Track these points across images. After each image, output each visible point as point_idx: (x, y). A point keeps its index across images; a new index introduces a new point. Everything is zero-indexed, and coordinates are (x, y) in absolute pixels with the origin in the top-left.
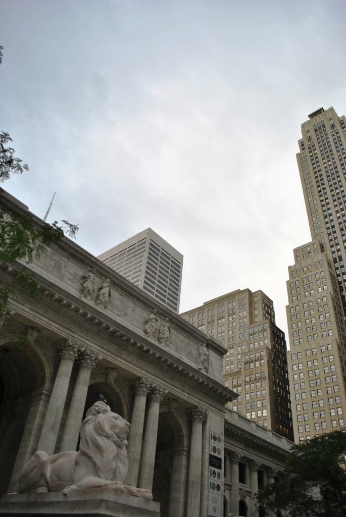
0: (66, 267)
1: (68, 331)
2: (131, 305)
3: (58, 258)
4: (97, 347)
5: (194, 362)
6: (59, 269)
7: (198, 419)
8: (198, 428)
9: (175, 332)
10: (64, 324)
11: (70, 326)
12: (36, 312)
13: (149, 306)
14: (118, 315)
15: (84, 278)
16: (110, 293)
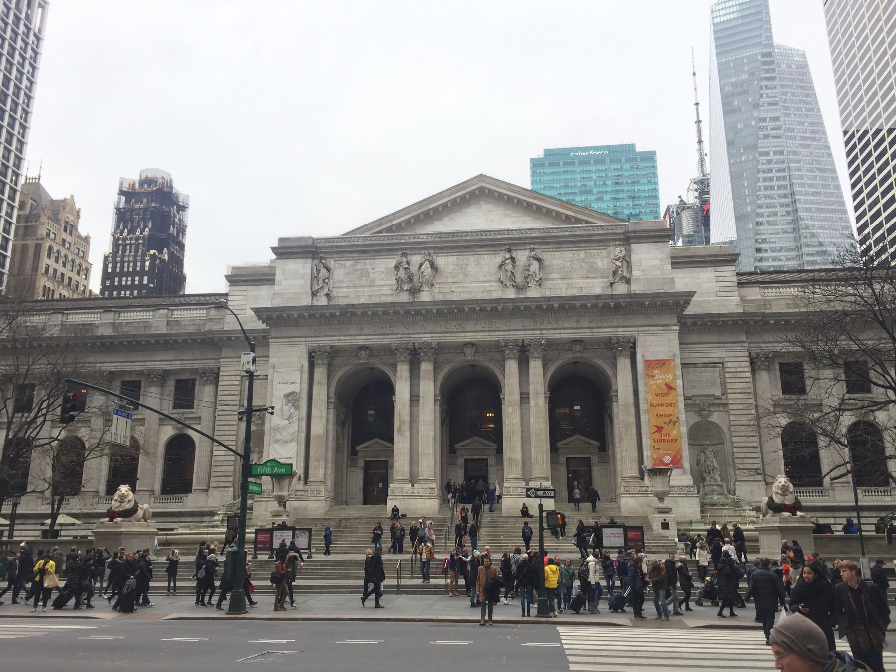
0: (374, 269)
1: (390, 336)
2: (472, 258)
3: (362, 264)
4: (429, 335)
5: (603, 277)
6: (367, 275)
7: (618, 353)
8: (624, 364)
9: (556, 253)
10: (384, 331)
11: (391, 329)
12: (352, 335)
13: (501, 245)
14: (454, 283)
15: (397, 268)
16: (433, 266)
